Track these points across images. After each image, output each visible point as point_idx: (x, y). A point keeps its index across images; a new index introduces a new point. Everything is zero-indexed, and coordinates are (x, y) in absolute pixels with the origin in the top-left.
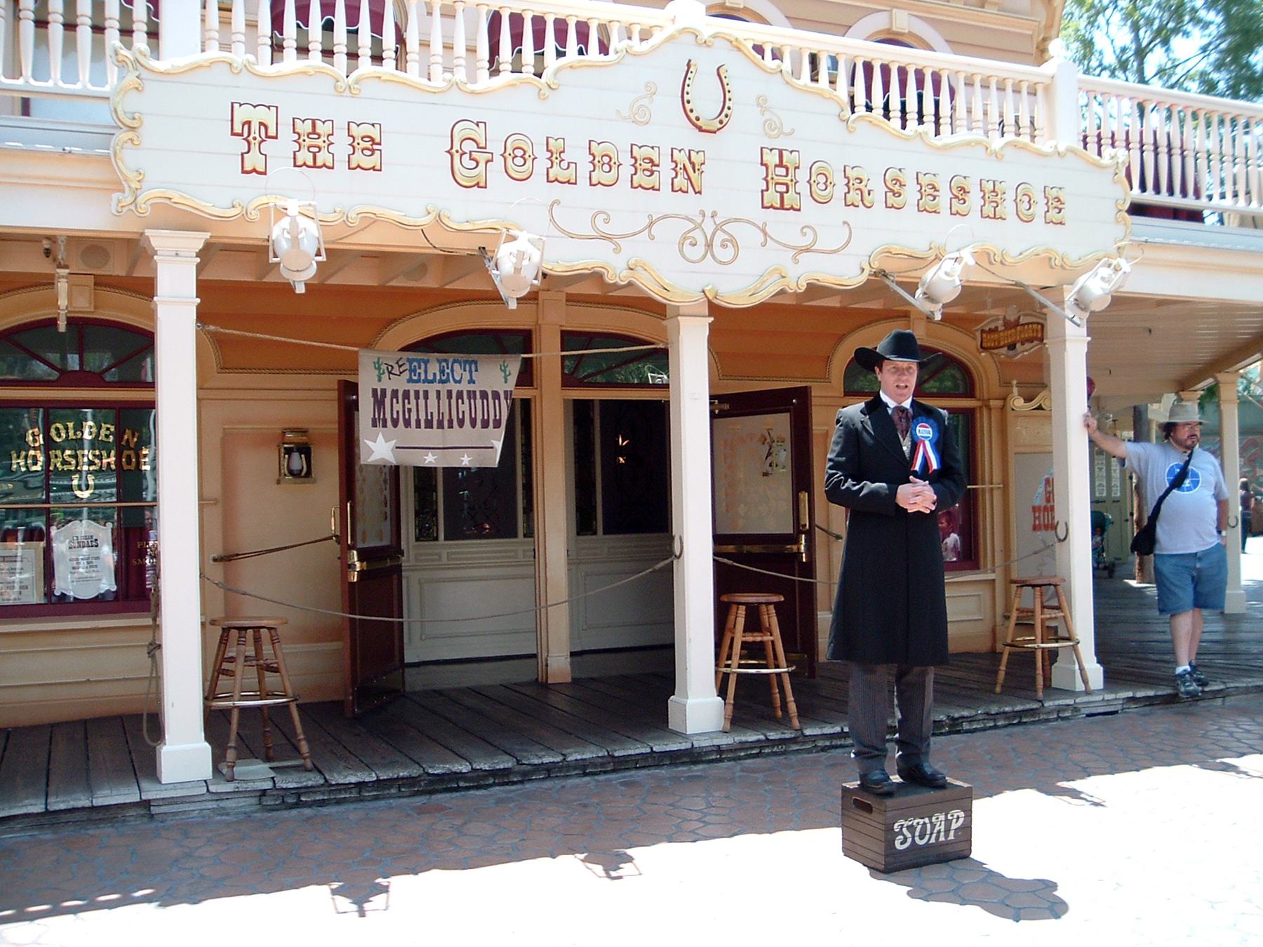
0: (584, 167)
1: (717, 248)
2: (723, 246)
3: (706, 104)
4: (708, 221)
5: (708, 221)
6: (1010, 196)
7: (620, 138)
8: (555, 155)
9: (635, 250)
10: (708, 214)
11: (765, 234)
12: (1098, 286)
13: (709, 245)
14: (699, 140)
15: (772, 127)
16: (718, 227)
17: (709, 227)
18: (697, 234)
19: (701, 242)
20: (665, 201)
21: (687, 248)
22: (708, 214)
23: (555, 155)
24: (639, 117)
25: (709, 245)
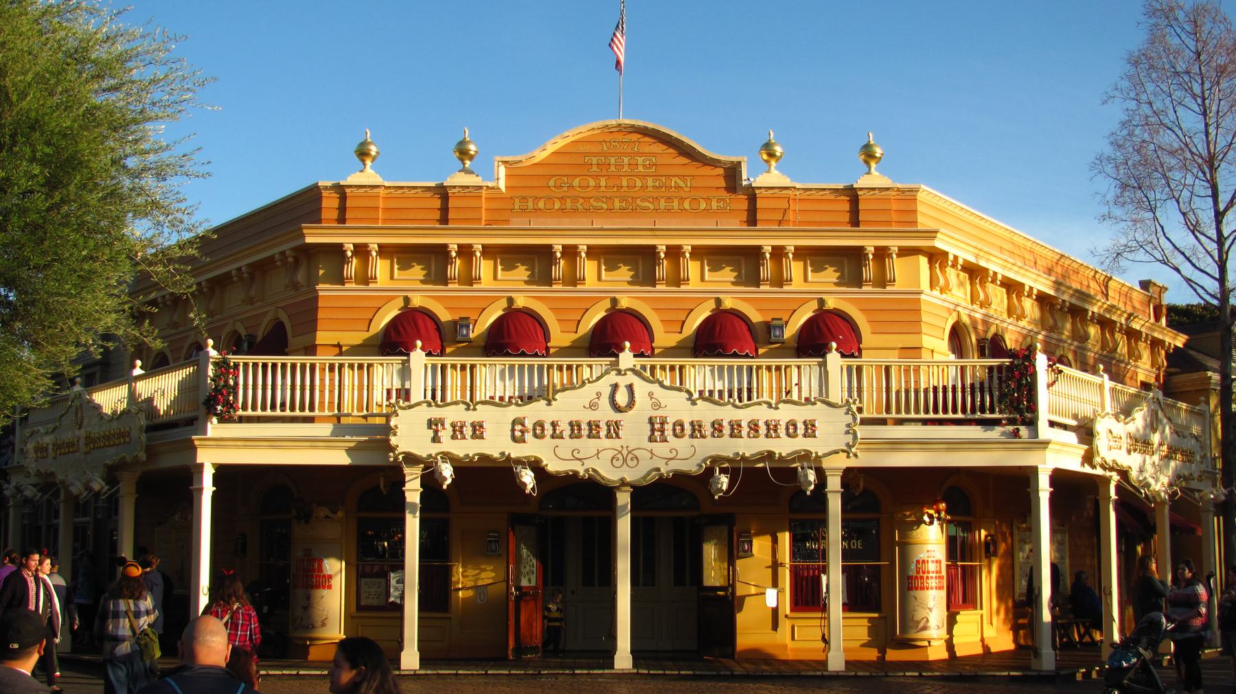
0: (567, 433)
1: (629, 462)
2: (632, 459)
3: (622, 398)
4: (625, 449)
5: (625, 449)
6: (784, 426)
7: (585, 417)
8: (554, 425)
9: (590, 464)
10: (625, 446)
11: (652, 453)
12: (842, 462)
13: (625, 460)
14: (616, 416)
15: (657, 406)
16: (630, 452)
17: (625, 452)
18: (619, 456)
19: (621, 457)
20: (604, 442)
21: (614, 461)
22: (625, 446)
23: (554, 425)
24: (593, 406)
25: (625, 460)
